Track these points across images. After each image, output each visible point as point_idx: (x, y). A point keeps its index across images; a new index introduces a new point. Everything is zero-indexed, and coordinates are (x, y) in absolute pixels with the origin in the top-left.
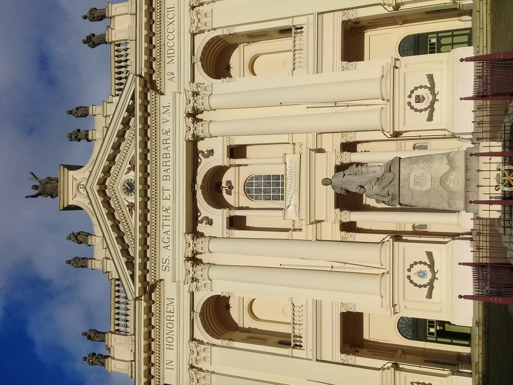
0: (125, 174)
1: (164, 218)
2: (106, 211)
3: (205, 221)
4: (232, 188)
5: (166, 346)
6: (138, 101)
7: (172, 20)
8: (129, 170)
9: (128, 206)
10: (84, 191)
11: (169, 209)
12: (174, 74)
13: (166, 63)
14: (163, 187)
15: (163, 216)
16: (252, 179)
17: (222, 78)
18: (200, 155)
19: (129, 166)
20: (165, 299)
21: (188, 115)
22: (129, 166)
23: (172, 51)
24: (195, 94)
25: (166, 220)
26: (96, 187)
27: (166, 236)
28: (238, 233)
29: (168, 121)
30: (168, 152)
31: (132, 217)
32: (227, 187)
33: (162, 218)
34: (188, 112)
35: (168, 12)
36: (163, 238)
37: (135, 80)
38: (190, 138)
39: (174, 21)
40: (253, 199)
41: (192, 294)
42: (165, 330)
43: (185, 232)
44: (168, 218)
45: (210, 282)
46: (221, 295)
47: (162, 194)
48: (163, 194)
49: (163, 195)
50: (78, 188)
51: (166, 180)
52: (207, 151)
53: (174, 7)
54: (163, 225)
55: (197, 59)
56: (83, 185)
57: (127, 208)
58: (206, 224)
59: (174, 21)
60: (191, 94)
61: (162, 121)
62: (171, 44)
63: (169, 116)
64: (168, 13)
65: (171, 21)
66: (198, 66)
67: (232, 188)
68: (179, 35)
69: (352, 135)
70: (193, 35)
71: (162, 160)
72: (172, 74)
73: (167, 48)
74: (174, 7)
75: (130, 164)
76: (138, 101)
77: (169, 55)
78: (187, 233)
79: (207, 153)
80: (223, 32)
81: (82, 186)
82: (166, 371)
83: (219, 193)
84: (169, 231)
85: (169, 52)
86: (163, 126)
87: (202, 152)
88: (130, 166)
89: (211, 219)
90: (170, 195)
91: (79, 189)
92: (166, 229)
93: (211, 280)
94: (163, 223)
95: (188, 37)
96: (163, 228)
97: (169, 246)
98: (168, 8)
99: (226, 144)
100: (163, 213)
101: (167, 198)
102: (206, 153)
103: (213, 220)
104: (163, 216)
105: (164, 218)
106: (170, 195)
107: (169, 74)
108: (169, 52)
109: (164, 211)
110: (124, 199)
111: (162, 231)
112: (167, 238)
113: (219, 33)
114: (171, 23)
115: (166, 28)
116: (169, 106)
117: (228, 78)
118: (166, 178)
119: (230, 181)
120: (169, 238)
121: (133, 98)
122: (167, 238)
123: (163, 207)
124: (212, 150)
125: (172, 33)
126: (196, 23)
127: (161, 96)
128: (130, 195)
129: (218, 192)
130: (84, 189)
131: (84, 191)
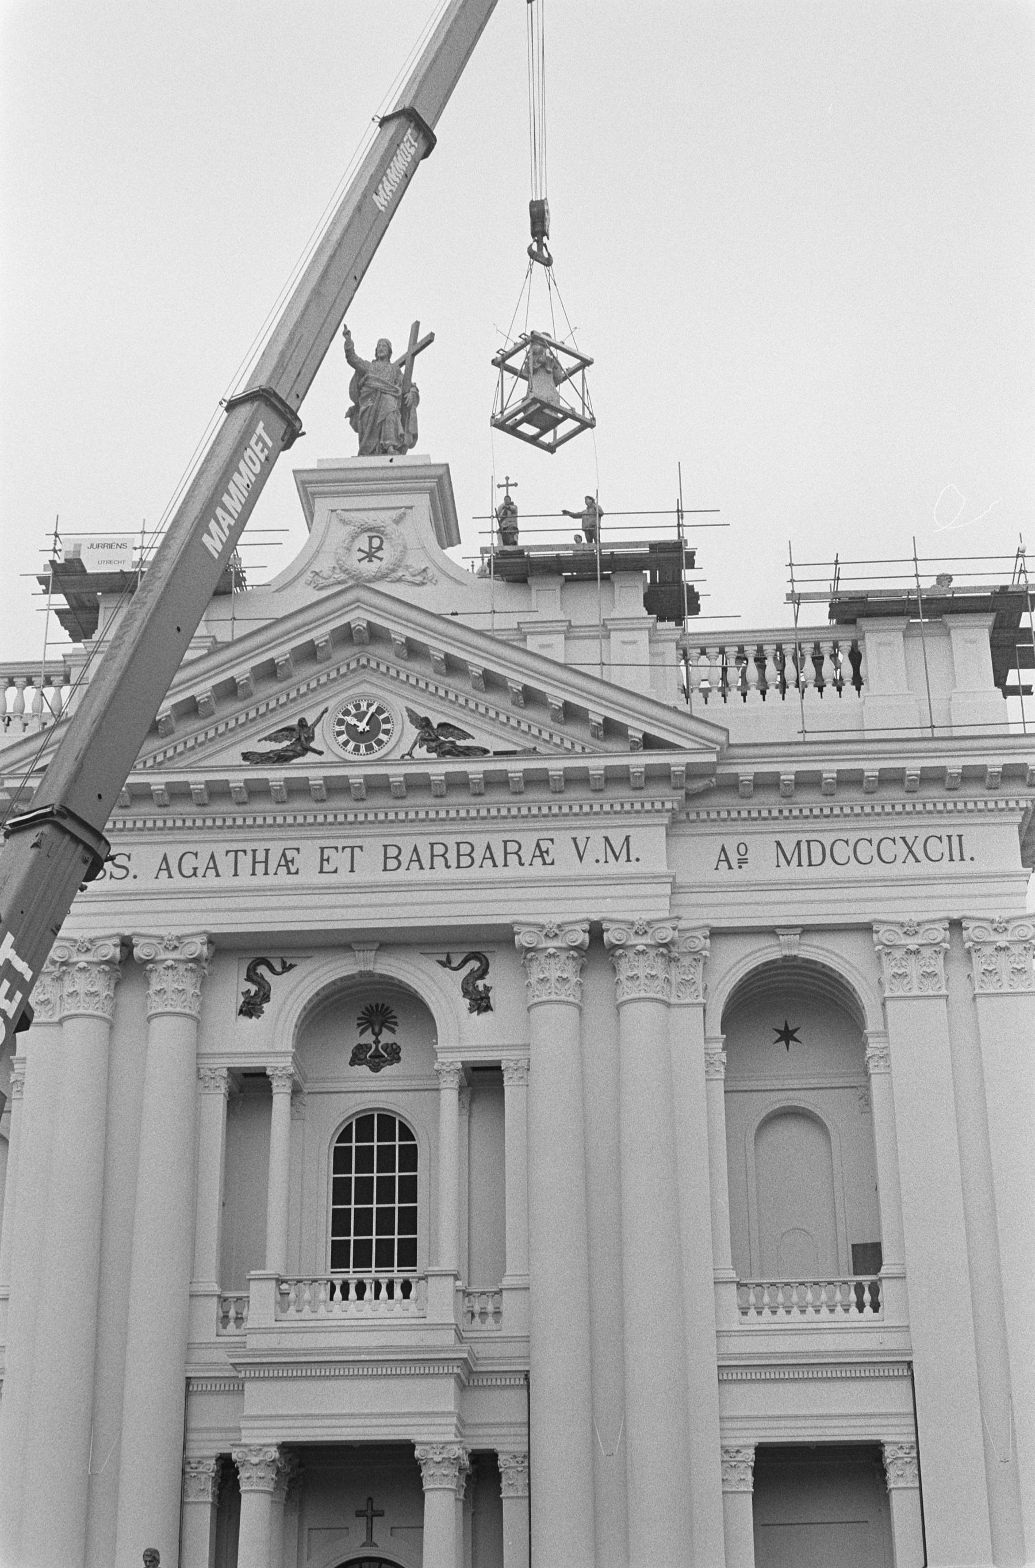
0: (408, 710)
1: (260, 856)
2: (281, 659)
3: (254, 989)
4: (376, 1069)
6: (640, 761)
7: (921, 855)
8: (424, 723)
9: (302, 723)
10: (360, 550)
11: (289, 873)
12: (740, 867)
13: (778, 837)
14: (361, 847)
15: (267, 851)
16: (407, 1133)
17: (725, 1036)
18: (474, 964)
21: (596, 931)
23: (817, 858)
24: (667, 951)
25: (254, 862)
26: (358, 618)
27: (202, 863)
28: (216, 1104)
29: (581, 858)
30: (477, 863)
31: (265, 739)
32: (377, 1048)
33: (261, 847)
34: (608, 930)
35: (949, 837)
36: (196, 854)
37: (708, 750)
38: (522, 939)
39: (917, 861)
40: (337, 1142)
44: (260, 868)
45: (56, 1019)
46: (14, 1054)
47: (340, 843)
48: (340, 850)
49: (336, 848)
50: (370, 530)
51: (386, 858)
52: (487, 989)
53: (962, 859)
54: (239, 853)
55: (790, 946)
56: (380, 548)
57: (294, 722)
58: (248, 991)
59: (917, 861)
60: (665, 939)
62: (842, 852)
63: (597, 861)
64: (945, 840)
65: (918, 849)
66: (768, 951)
67: (376, 1069)
68: (871, 882)
69: (520, 1489)
71: (451, 841)
72: (742, 861)
73: (828, 839)
74: (962, 859)
75: (441, 725)
76: (640, 761)
77: (804, 847)
78: (212, 940)
79: (481, 988)
80: (877, 1034)
81: (376, 543)
83: (360, 1022)
84: (218, 875)
85: (816, 849)
86: (563, 839)
87: (483, 973)
88: (435, 726)
89: (263, 1012)
90: (335, 871)
91: (365, 531)
92: (225, 864)
93: (60, 1023)
94: (245, 851)
96: (228, 852)
97: (170, 876)
98: (960, 836)
99: (506, 1059)
101: (325, 863)
102: (480, 984)
103: (258, 1017)
104: (267, 851)
105: (260, 856)
106: (335, 871)
107: (742, 847)
108: (816, 849)
109: (284, 855)
110: (326, 710)
111: (219, 850)
112: (195, 869)
113: (872, 1024)
114: (911, 851)
115: (897, 834)
116: (629, 860)
117: (724, 1058)
118: (390, 859)
119: (399, 1059)
120: (195, 874)
121: (650, 743)
122: (195, 869)
123: (298, 850)
124: (488, 1008)
125: (876, 858)
126: (905, 940)
127: (662, 831)
128: (338, 728)
129: (361, 1015)
130: (367, 550)
131: (360, 550)
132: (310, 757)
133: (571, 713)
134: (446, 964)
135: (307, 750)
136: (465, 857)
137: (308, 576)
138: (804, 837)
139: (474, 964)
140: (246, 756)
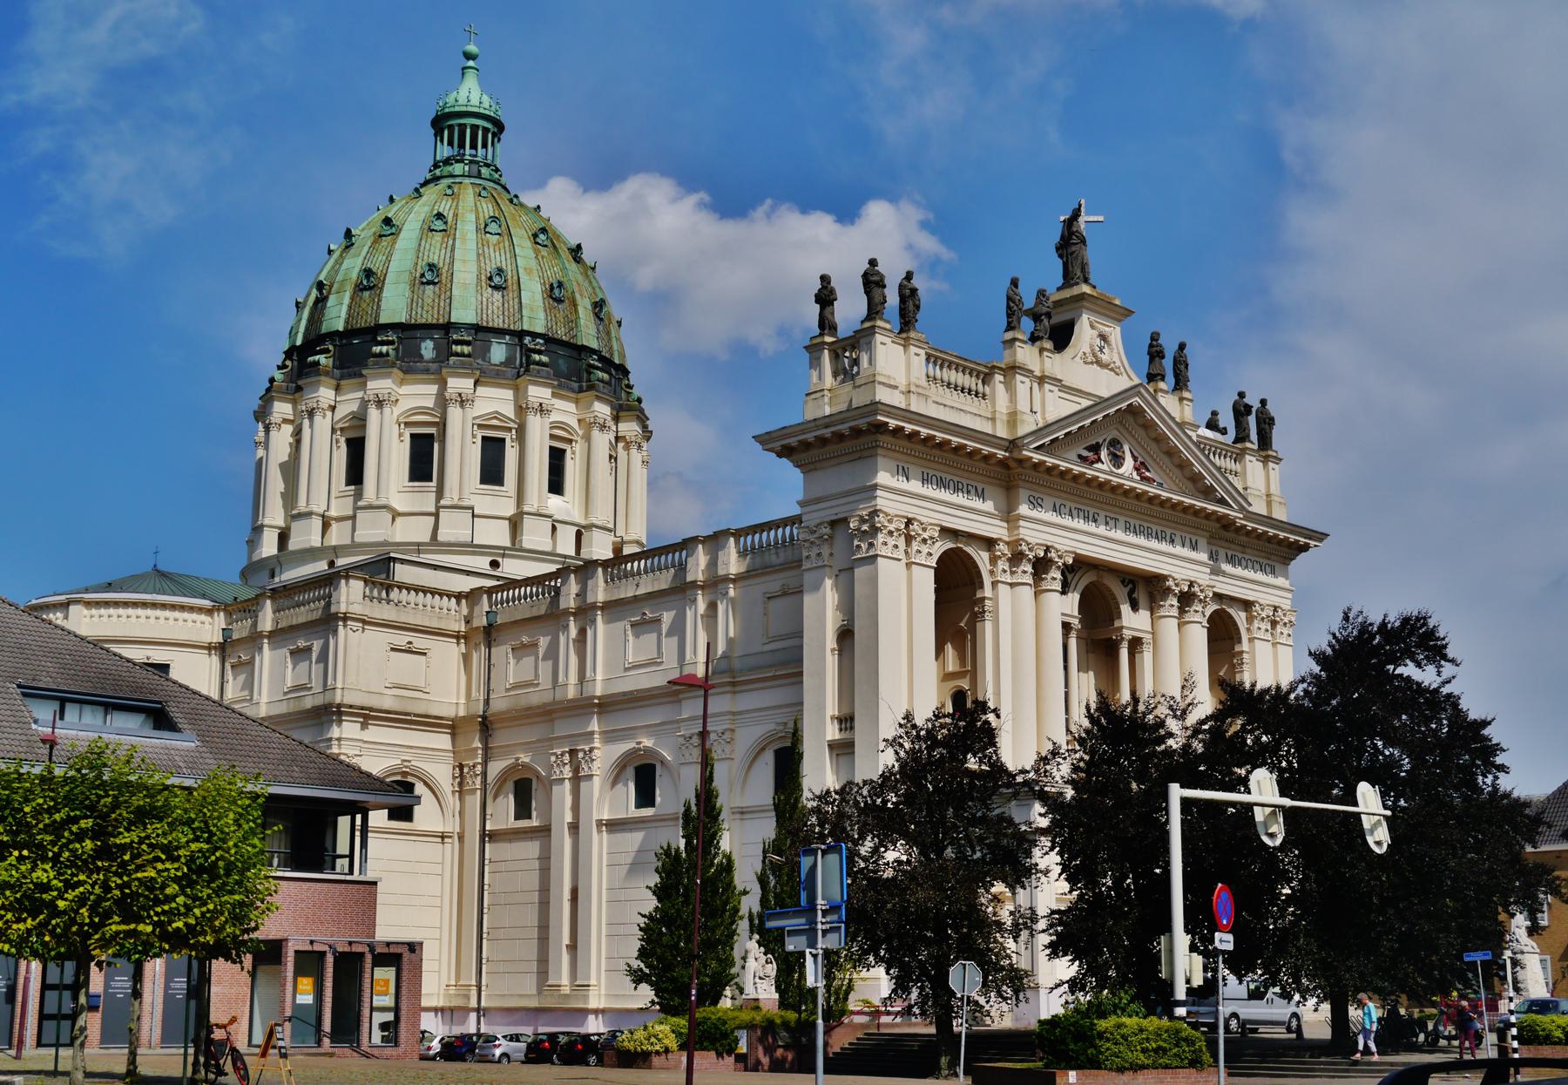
5: (926, 471)
9: (1097, 443)
18: (1130, 586)
19: (1140, 459)
20: (984, 486)
22: (1140, 459)
27: (1067, 511)
33: (1087, 509)
38: (1170, 583)
41: (989, 543)
42: (947, 475)
43: (1078, 551)
61: (1183, 535)
70: (1247, 605)
71: (1146, 525)
82: (896, 463)
86: (1178, 534)
95: (1250, 596)
100: (1092, 511)
121: (1222, 502)
132: (1099, 465)
133: (1196, 479)
134: (1123, 582)
135: (1099, 460)
136: (1149, 536)
137: (1079, 355)
138: (1234, 553)
139: (1130, 586)
140: (1080, 456)
